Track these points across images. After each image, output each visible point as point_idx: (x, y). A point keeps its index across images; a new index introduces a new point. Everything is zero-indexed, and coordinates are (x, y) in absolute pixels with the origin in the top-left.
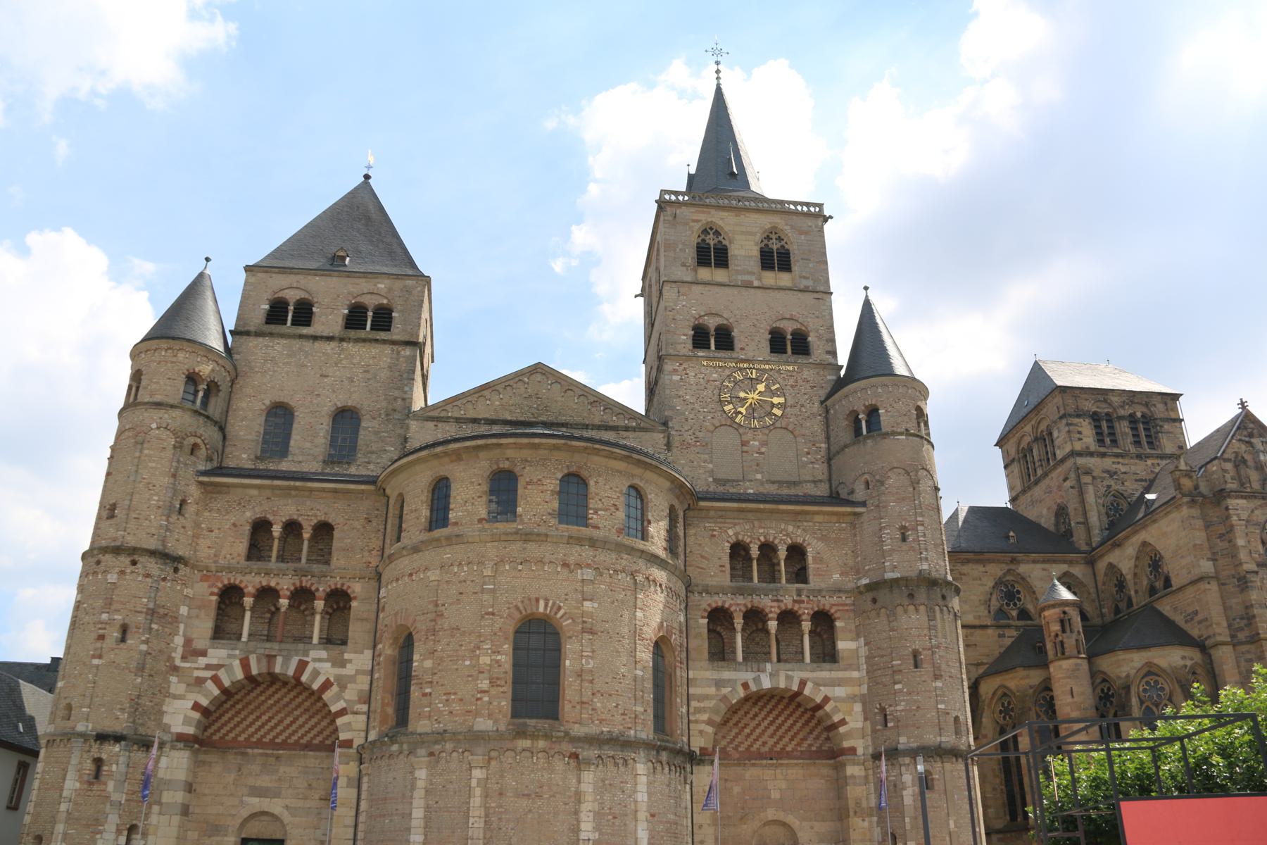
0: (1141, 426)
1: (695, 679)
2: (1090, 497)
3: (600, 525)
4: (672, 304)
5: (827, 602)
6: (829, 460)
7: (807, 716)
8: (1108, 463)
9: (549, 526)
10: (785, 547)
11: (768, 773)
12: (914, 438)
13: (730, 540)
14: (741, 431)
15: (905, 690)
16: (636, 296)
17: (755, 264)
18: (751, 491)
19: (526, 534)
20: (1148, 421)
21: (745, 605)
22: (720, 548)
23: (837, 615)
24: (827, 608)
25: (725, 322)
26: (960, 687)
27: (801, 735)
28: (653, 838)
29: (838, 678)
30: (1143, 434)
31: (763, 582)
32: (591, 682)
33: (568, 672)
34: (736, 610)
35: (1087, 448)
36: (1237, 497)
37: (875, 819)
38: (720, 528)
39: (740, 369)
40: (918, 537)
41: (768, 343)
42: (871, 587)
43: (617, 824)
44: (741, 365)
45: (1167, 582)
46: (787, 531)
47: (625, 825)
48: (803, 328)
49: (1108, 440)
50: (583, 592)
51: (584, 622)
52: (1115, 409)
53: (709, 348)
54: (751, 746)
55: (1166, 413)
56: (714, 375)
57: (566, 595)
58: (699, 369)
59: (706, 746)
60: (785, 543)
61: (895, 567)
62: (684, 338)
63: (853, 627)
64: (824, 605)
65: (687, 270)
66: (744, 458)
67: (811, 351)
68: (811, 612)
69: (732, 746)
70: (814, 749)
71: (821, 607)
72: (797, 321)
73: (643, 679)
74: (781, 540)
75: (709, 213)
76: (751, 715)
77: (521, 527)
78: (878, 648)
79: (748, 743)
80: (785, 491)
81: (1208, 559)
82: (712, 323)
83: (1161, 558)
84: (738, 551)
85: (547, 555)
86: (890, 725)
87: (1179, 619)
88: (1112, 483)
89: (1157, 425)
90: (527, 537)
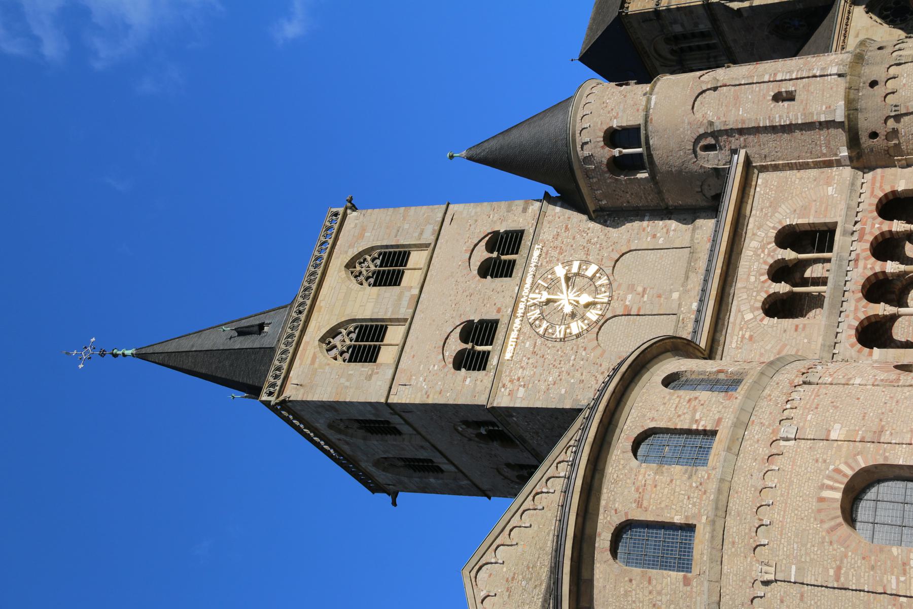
3: (717, 417)
4: (419, 395)
5: (869, 202)
9: (708, 478)
16: (394, 503)
17: (388, 292)
19: (717, 508)
21: (858, 300)
23: (888, 189)
24: (876, 201)
25: (459, 330)
34: (864, 312)
38: (741, 329)
46: (757, 249)
48: (487, 238)
53: (489, 352)
56: (527, 345)
60: (774, 251)
64: (870, 205)
65: (377, 373)
71: (874, 207)
72: (476, 245)
74: (769, 255)
75: (308, 343)
77: (704, 518)
82: (456, 345)
90: (722, 510)
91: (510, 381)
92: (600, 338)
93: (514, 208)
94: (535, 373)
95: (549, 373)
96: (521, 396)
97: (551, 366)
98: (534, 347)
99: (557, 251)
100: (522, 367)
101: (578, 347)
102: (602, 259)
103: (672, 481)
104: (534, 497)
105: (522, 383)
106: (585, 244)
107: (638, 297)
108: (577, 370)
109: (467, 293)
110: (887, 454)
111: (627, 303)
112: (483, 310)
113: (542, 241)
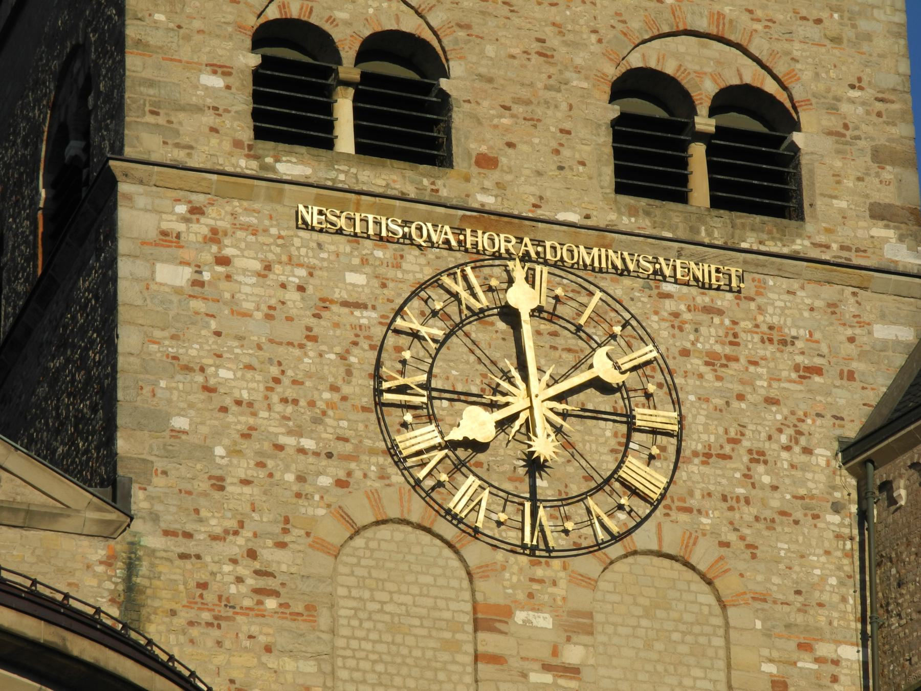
14: (475, 552)
39: (479, 259)
41: (605, 139)
44: (483, 240)
48: (770, 86)
53: (328, 144)
56: (356, 279)
58: (284, 242)
91: (214, 231)
92: (384, 532)
93: (889, 173)
94: (247, 315)
95: (249, 367)
96: (159, 278)
97: (275, 371)
98: (345, 304)
99: (718, 348)
100: (268, 268)
102: (689, 510)
105: (206, 276)
106: (746, 443)
107: (545, 654)
108: (261, 465)
109: (554, 41)
111: (520, 616)
112: (486, 104)
113: (761, 290)
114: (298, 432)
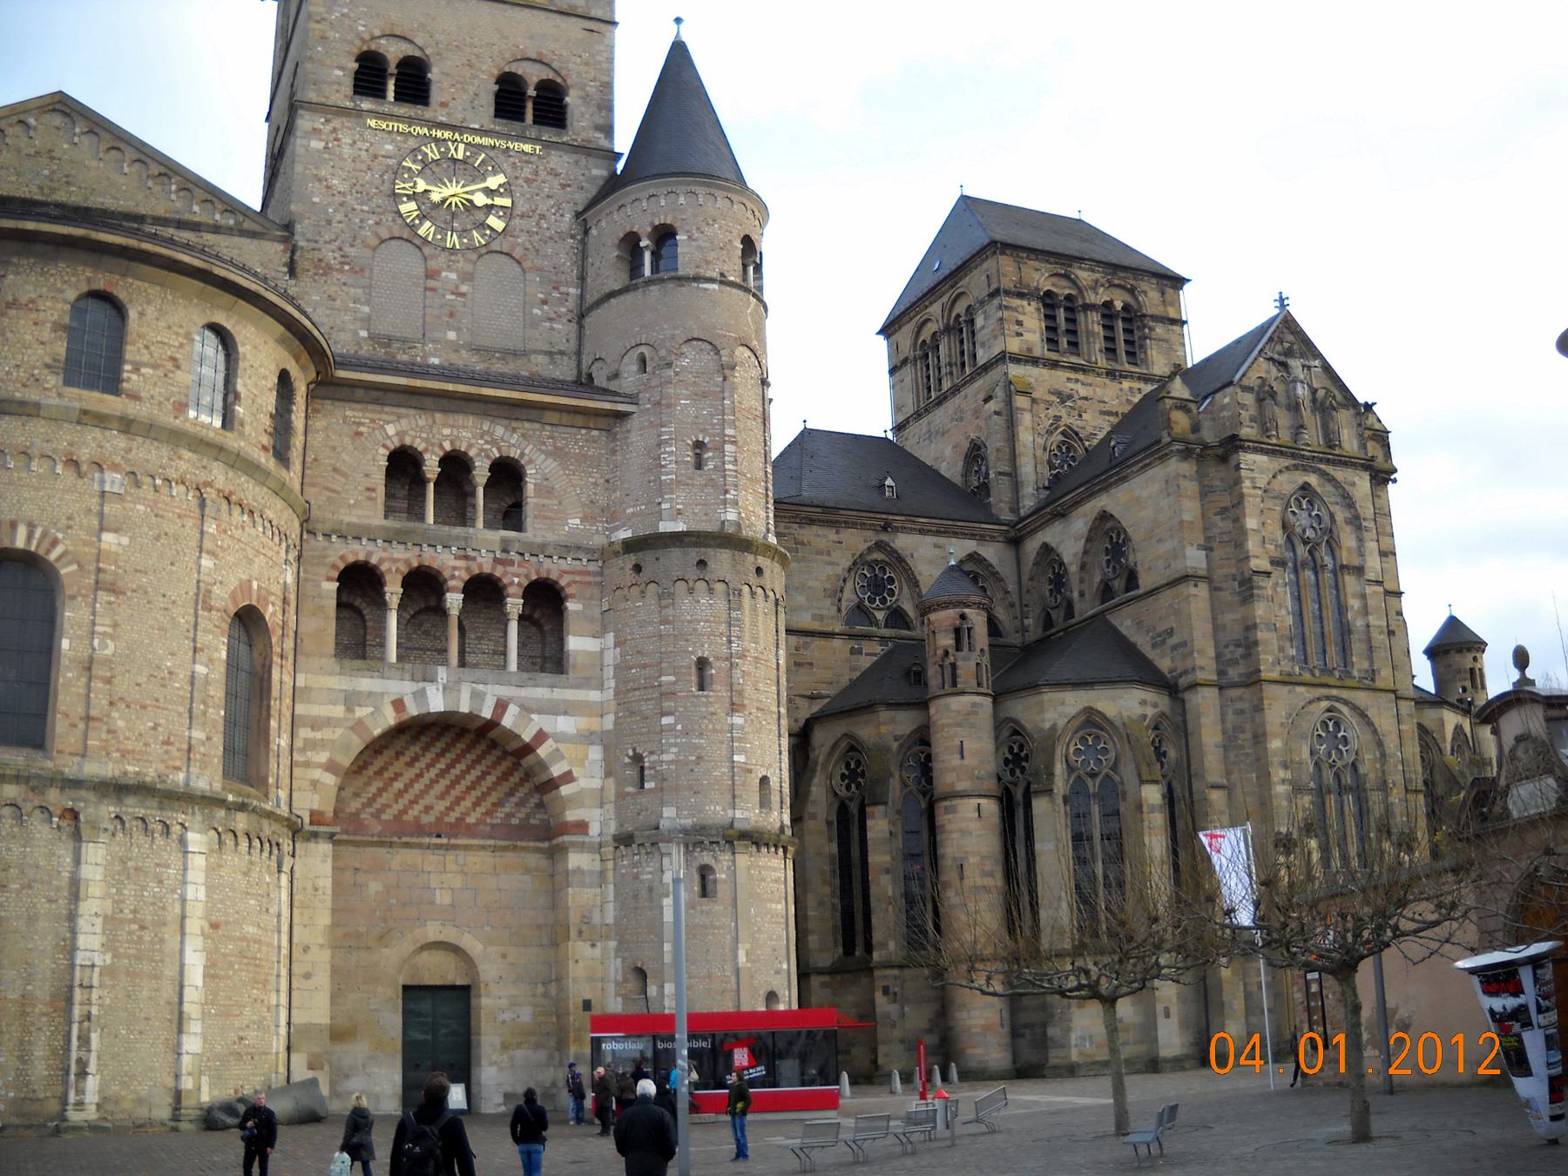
0: (1120, 324)
1: (307, 689)
2: (1025, 437)
4: (322, 10)
5: (554, 568)
6: (582, 316)
7: (506, 764)
8: (1060, 378)
9: (45, 389)
10: (487, 464)
11: (432, 860)
12: (734, 291)
13: (388, 443)
14: (427, 251)
15: (679, 727)
18: (436, 361)
20: (1133, 318)
21: (407, 562)
22: (370, 456)
23: (569, 591)
24: (554, 576)
25: (417, 53)
26: (775, 728)
27: (493, 798)
28: (214, 965)
29: (564, 701)
30: (1121, 337)
31: (444, 523)
32: (109, 681)
33: (64, 662)
34: (390, 570)
35: (1029, 350)
36: (1256, 450)
37: (613, 944)
38: (373, 421)
39: (437, 140)
40: (724, 463)
42: (630, 546)
43: (147, 938)
44: (439, 134)
45: (1132, 579)
47: (162, 941)
48: (559, 80)
49: (1064, 342)
50: (101, 515)
51: (99, 570)
52: (1080, 291)
54: (405, 811)
55: (1161, 308)
56: (389, 147)
57: (70, 518)
59: (322, 809)
60: (488, 457)
61: (679, 512)
62: (338, 75)
63: (597, 611)
66: (427, 301)
67: (568, 122)
68: (526, 583)
69: (369, 810)
70: (515, 821)
73: (207, 682)
74: (482, 450)
76: (406, 758)
78: (639, 652)
79: (399, 806)
80: (498, 367)
81: (1200, 547)
82: (394, 52)
83: (1127, 539)
84: (403, 464)
85: (38, 441)
86: (647, 786)
87: (1142, 642)
88: (1063, 413)
89: (1145, 326)
101: (379, 214)
103: (43, 343)
104: (165, 174)
107: (453, 289)
109: (474, 61)
110: (80, 599)
111: (444, 274)
114: (362, 204)
